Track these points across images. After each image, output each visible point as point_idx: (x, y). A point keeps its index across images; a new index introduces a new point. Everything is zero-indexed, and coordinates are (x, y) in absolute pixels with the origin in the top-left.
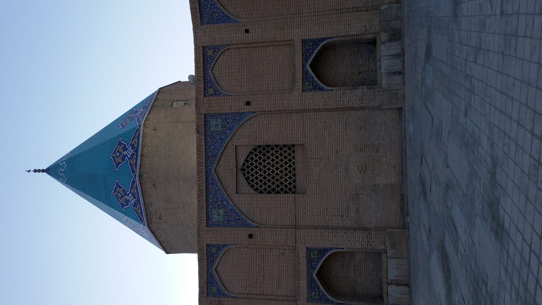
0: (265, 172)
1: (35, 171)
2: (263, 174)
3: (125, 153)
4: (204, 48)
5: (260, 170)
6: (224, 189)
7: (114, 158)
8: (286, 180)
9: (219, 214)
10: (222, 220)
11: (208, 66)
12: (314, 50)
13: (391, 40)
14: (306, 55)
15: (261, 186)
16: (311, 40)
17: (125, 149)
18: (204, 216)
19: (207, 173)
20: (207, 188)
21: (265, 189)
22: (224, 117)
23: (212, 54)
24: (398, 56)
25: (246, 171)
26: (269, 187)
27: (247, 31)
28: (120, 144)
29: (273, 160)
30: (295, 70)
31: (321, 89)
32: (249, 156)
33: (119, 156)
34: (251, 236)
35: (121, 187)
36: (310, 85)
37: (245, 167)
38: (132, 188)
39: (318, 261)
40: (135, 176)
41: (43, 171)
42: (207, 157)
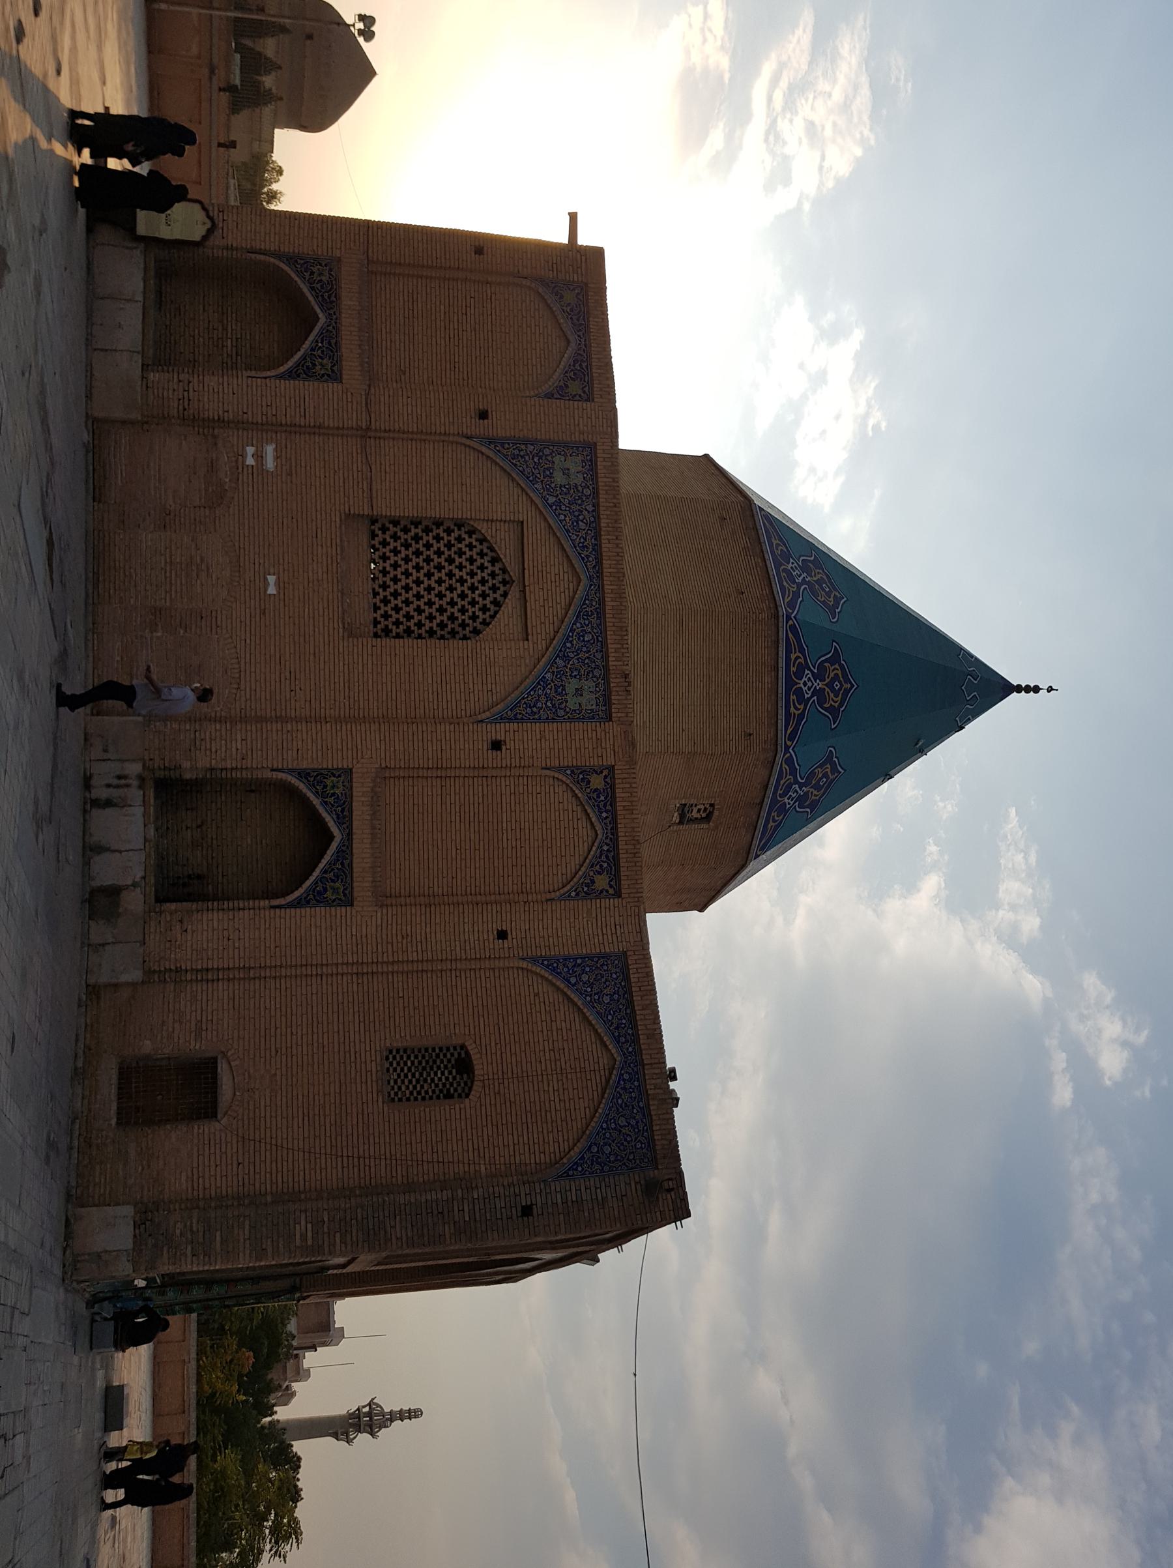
0: (450, 575)
1: (1036, 689)
2: (456, 571)
3: (819, 685)
4: (618, 894)
5: (462, 581)
6: (555, 534)
7: (847, 681)
8: (396, 552)
9: (566, 472)
10: (557, 459)
11: (605, 848)
12: (321, 879)
13: (114, 892)
14: (342, 864)
15: (460, 539)
16: (330, 904)
18: (601, 472)
19: (600, 575)
20: (597, 536)
21: (449, 531)
22: (561, 713)
23: (598, 878)
24: (99, 849)
25: (500, 578)
26: (438, 538)
27: (502, 935)
28: (834, 711)
29: (430, 604)
30: (373, 828)
31: (303, 775)
32: (493, 617)
34: (483, 415)
35: (824, 602)
36: (333, 787)
37: (502, 589)
38: (796, 595)
39: (313, 350)
40: (789, 618)
41: (1019, 689)
42: (601, 615)
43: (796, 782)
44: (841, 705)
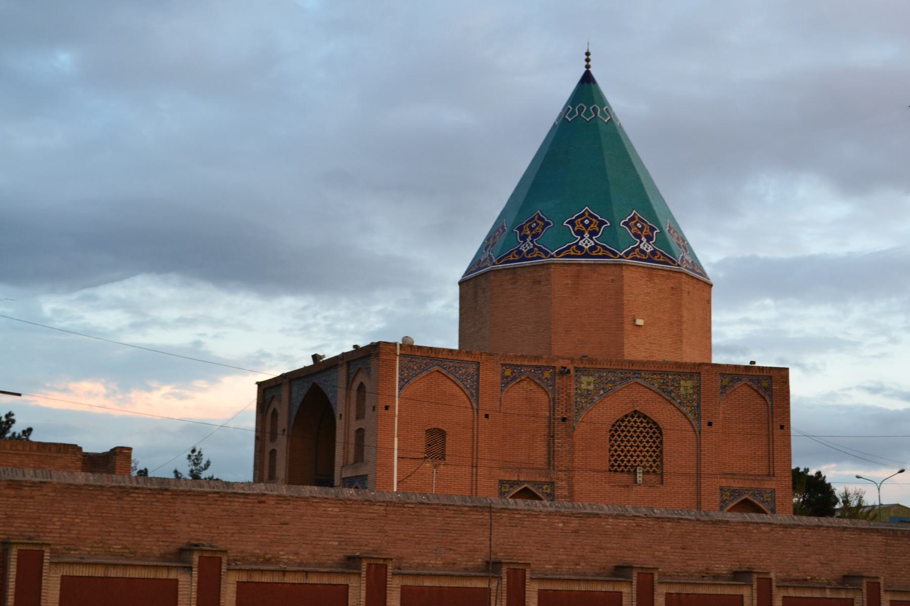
3: (587, 235)
7: (583, 214)
17: (593, 233)
33: (584, 225)
38: (540, 249)
41: (588, 67)
43: (639, 246)
44: (596, 218)
